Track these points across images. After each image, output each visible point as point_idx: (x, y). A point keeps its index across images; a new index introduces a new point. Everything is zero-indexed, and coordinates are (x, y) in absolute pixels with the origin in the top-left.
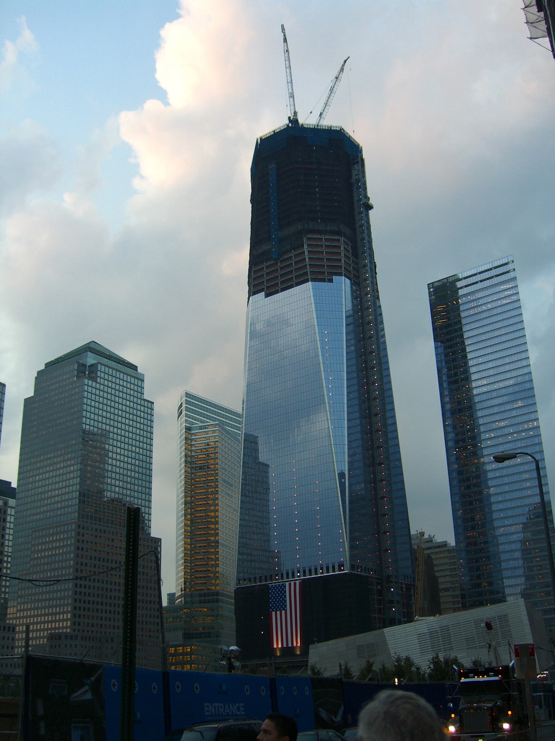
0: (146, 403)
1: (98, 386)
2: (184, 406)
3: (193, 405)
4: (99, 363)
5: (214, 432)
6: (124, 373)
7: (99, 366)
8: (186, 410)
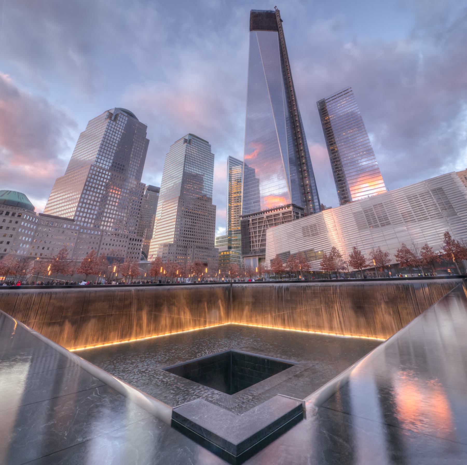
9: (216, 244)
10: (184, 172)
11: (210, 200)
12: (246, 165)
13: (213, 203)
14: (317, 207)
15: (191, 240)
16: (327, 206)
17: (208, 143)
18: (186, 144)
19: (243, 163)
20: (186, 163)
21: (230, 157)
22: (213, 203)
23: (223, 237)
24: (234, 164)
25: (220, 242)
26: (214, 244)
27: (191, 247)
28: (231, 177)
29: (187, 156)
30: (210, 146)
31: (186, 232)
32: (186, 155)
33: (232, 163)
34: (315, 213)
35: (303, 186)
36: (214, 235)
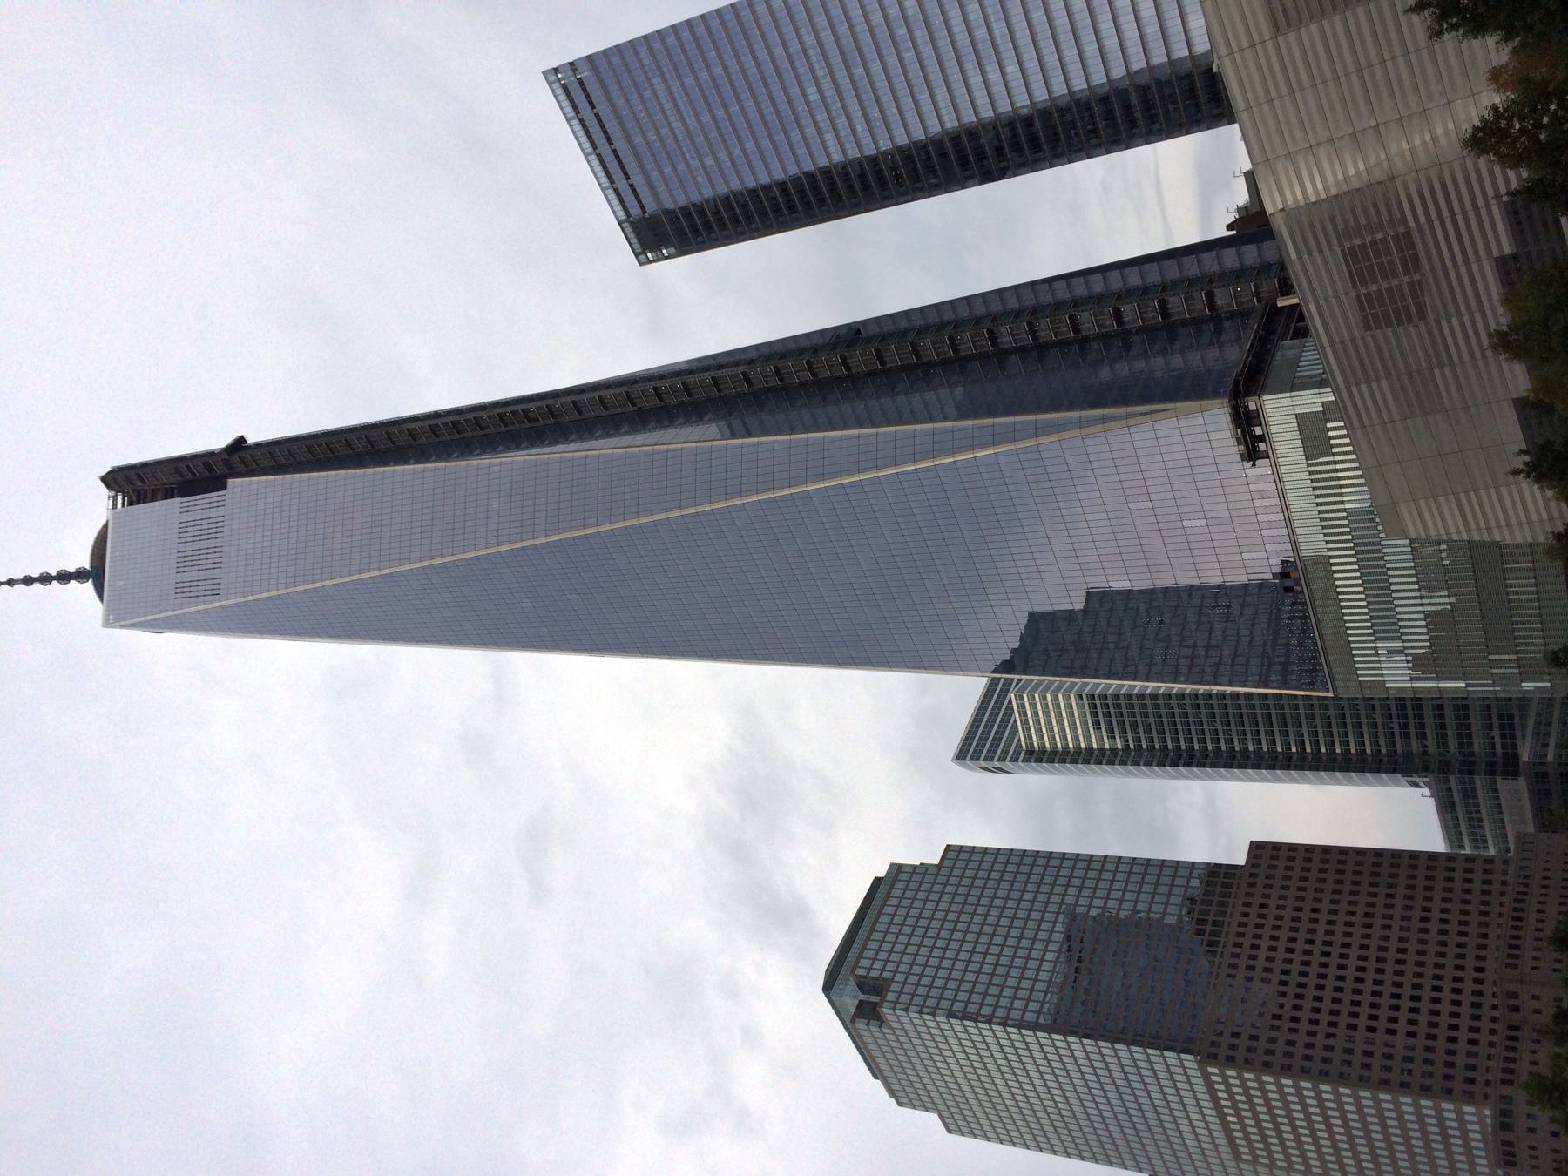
0: (947, 863)
1: (899, 977)
2: (984, 764)
3: (987, 743)
4: (853, 972)
5: (1034, 706)
6: (880, 912)
7: (861, 972)
8: (992, 759)
9: (1492, 851)
10: (1049, 1029)
11: (1216, 873)
12: (1006, 667)
13: (1240, 859)
14: (1251, 254)
15: (1467, 999)
16: (1242, 196)
17: (877, 881)
18: (886, 1011)
19: (993, 684)
20: (1000, 1012)
21: (960, 757)
22: (1240, 859)
23: (1447, 808)
24: (1000, 733)
25: (1476, 824)
26: (1488, 860)
27: (1515, 996)
28: (1078, 750)
29: (958, 1006)
30: (896, 870)
31: (1422, 1029)
32: (950, 1014)
33: (994, 745)
34: (1283, 268)
35: (1121, 339)
36: (1432, 856)
